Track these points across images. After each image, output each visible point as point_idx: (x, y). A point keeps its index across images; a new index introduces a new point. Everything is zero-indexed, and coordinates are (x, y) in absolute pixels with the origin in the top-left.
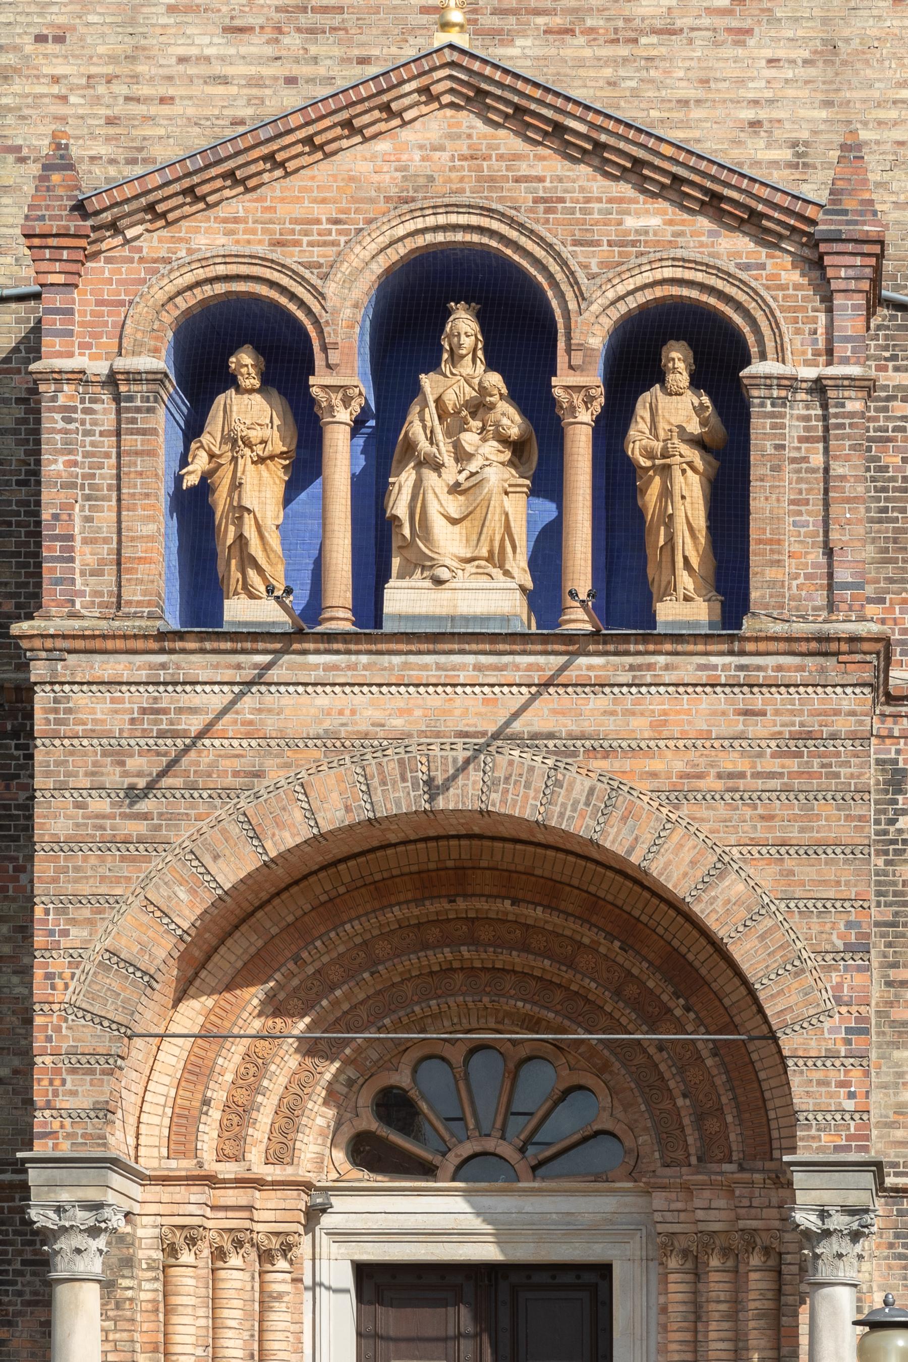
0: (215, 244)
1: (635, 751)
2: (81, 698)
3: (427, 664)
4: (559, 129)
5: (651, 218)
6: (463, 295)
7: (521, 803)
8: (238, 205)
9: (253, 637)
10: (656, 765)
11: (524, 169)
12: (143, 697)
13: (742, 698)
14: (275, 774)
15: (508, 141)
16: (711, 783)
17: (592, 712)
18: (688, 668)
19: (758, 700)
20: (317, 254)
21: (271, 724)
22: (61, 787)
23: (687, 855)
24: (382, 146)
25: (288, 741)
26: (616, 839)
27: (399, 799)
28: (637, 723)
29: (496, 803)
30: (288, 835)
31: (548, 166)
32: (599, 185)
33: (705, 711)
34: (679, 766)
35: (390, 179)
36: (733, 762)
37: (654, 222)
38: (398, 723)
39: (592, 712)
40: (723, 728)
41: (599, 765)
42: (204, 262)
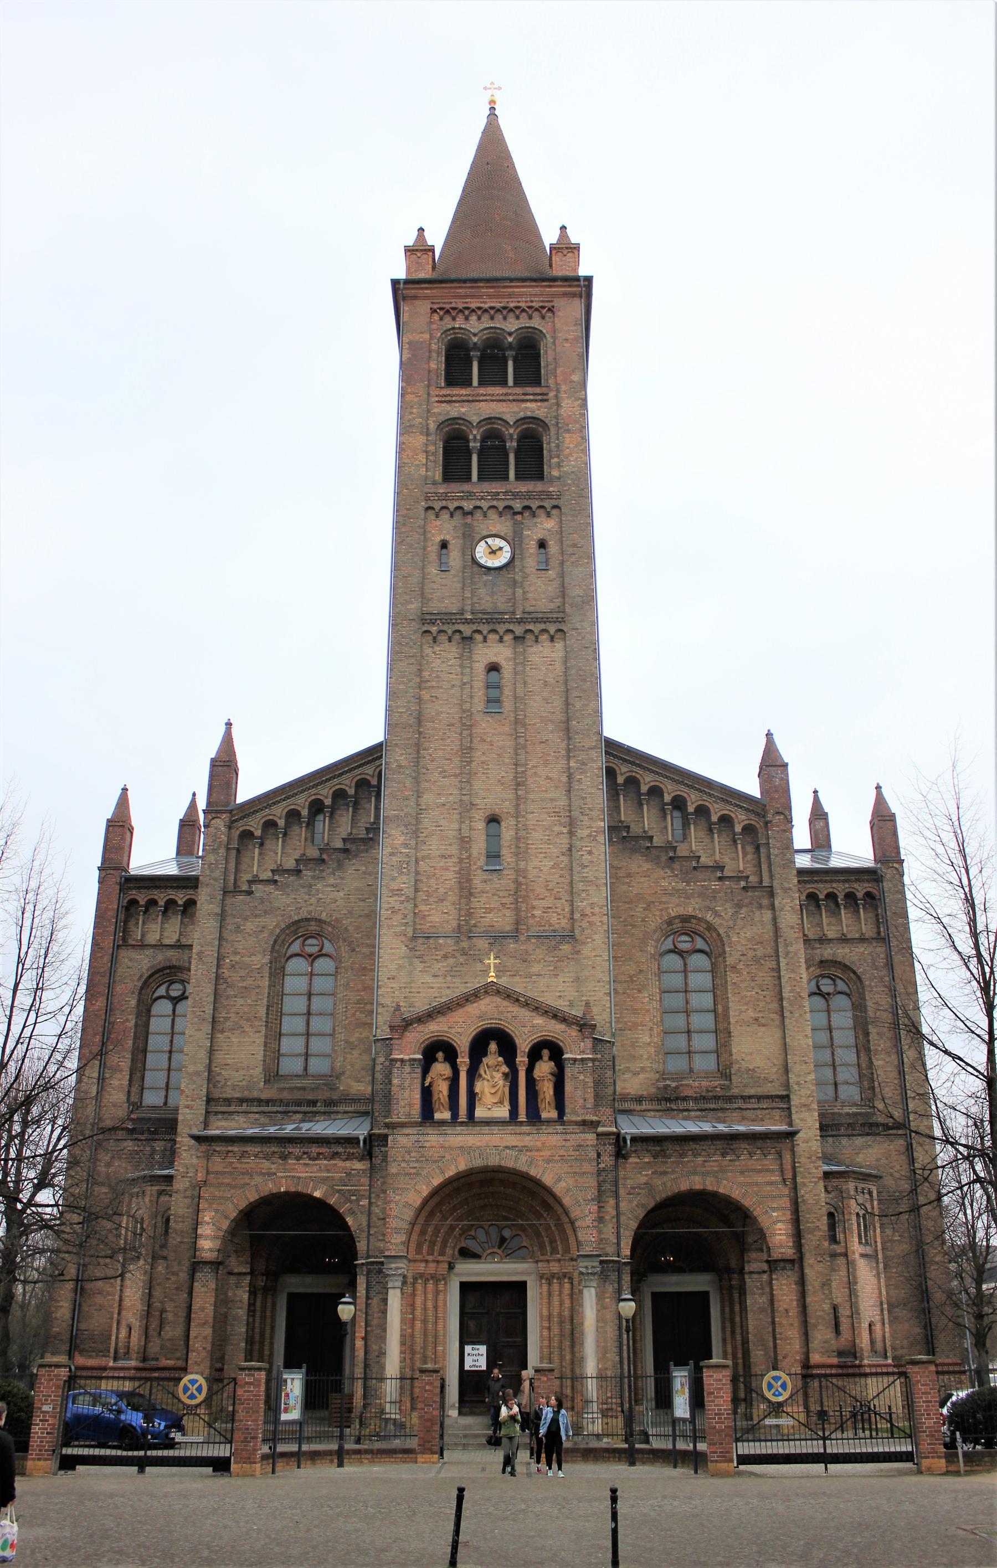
0: (435, 1029)
1: (538, 1150)
2: (400, 1138)
3: (486, 1129)
4: (518, 1000)
5: (539, 1021)
6: (493, 1039)
7: (509, 1164)
8: (441, 1019)
9: (442, 1123)
10: (543, 1154)
11: (509, 1009)
12: (415, 1138)
13: (564, 1137)
14: (448, 1157)
15: (505, 1003)
16: (557, 1158)
17: (527, 1141)
18: (551, 1130)
19: (568, 1137)
20: (459, 1030)
21: (447, 1144)
22: (395, 1160)
23: (551, 1176)
24: (475, 1005)
25: (451, 1148)
26: (533, 1172)
27: (478, 1163)
28: (539, 1144)
29: (503, 1163)
30: (451, 1173)
31: (516, 1009)
32: (527, 1013)
33: (555, 1140)
34: (549, 1153)
35: (477, 1012)
36: (562, 1152)
37: (540, 1022)
38: (479, 1144)
39: (527, 1141)
40: (559, 1144)
41: (528, 1154)
42: (432, 1032)
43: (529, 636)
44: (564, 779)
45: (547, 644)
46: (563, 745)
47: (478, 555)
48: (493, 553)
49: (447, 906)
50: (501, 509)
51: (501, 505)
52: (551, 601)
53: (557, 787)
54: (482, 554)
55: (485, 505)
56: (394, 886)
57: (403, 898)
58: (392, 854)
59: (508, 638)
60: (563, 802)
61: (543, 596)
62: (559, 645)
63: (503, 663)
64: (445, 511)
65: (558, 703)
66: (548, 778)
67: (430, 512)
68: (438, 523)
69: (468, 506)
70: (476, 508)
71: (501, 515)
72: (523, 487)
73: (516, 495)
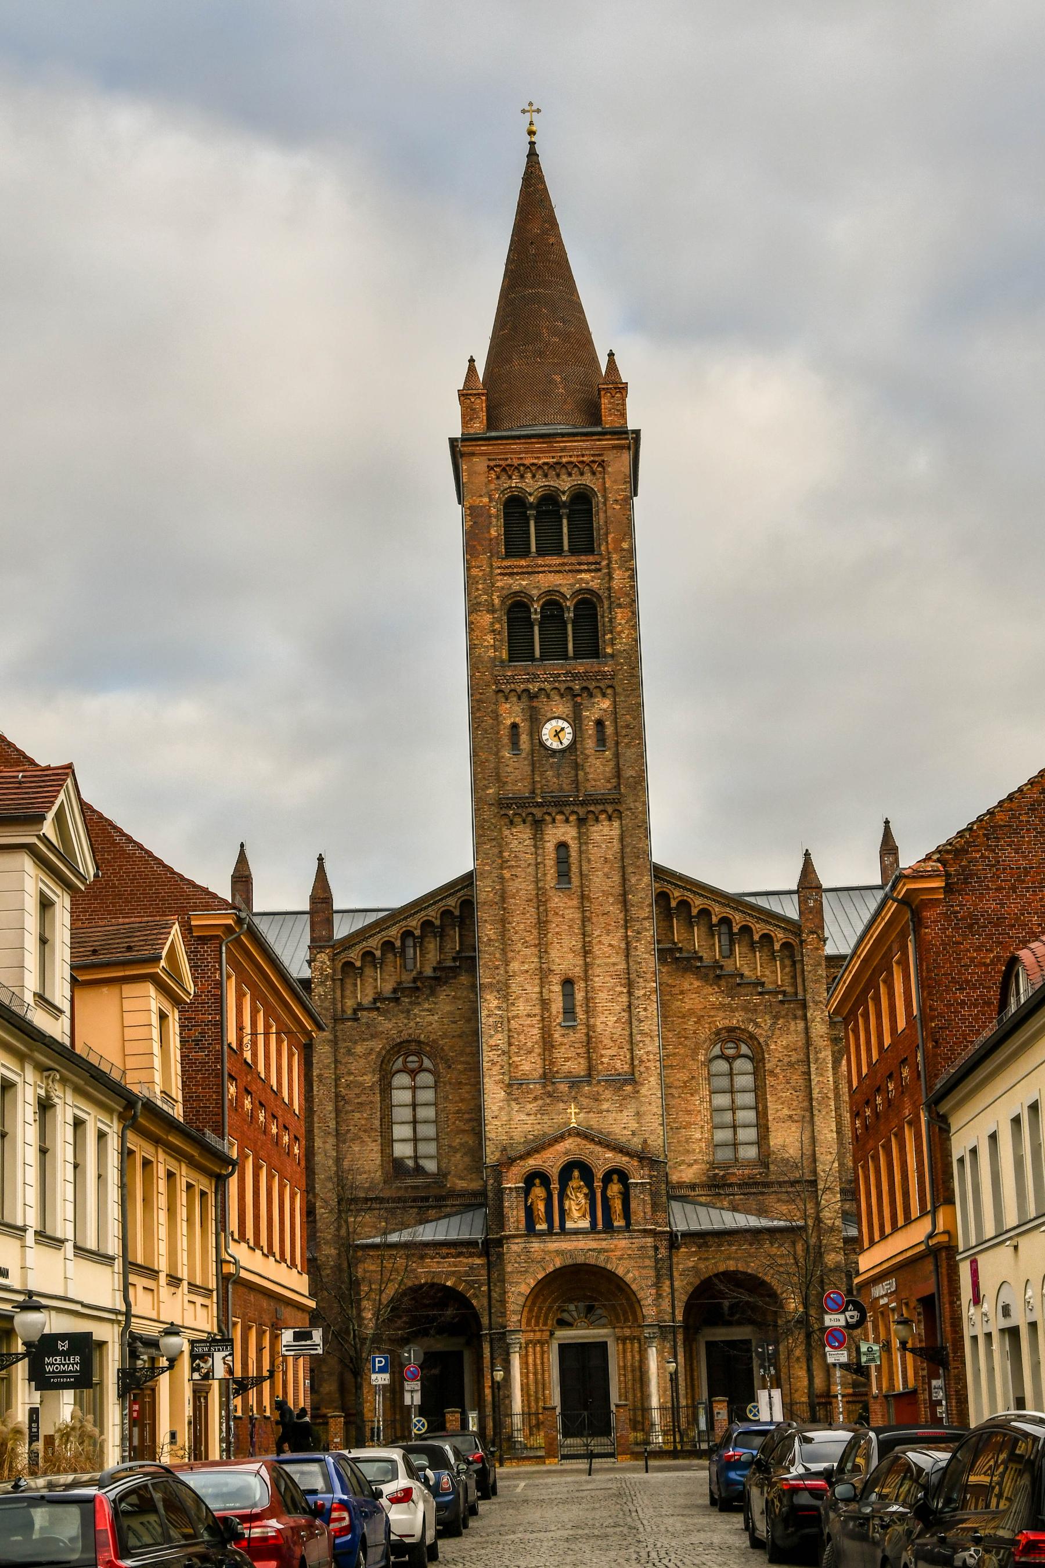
43: (590, 816)
44: (623, 946)
45: (606, 823)
46: (621, 916)
47: (544, 738)
48: (557, 732)
49: (535, 1057)
50: (562, 691)
51: (562, 687)
52: (608, 782)
53: (618, 953)
54: (547, 737)
55: (547, 686)
56: (492, 1042)
57: (500, 1052)
58: (489, 1016)
59: (572, 818)
60: (622, 966)
61: (601, 777)
62: (616, 824)
63: (570, 842)
64: (513, 694)
65: (617, 878)
66: (610, 945)
67: (501, 695)
68: (508, 706)
69: (533, 688)
70: (540, 689)
71: (562, 696)
72: (581, 666)
73: (576, 677)
